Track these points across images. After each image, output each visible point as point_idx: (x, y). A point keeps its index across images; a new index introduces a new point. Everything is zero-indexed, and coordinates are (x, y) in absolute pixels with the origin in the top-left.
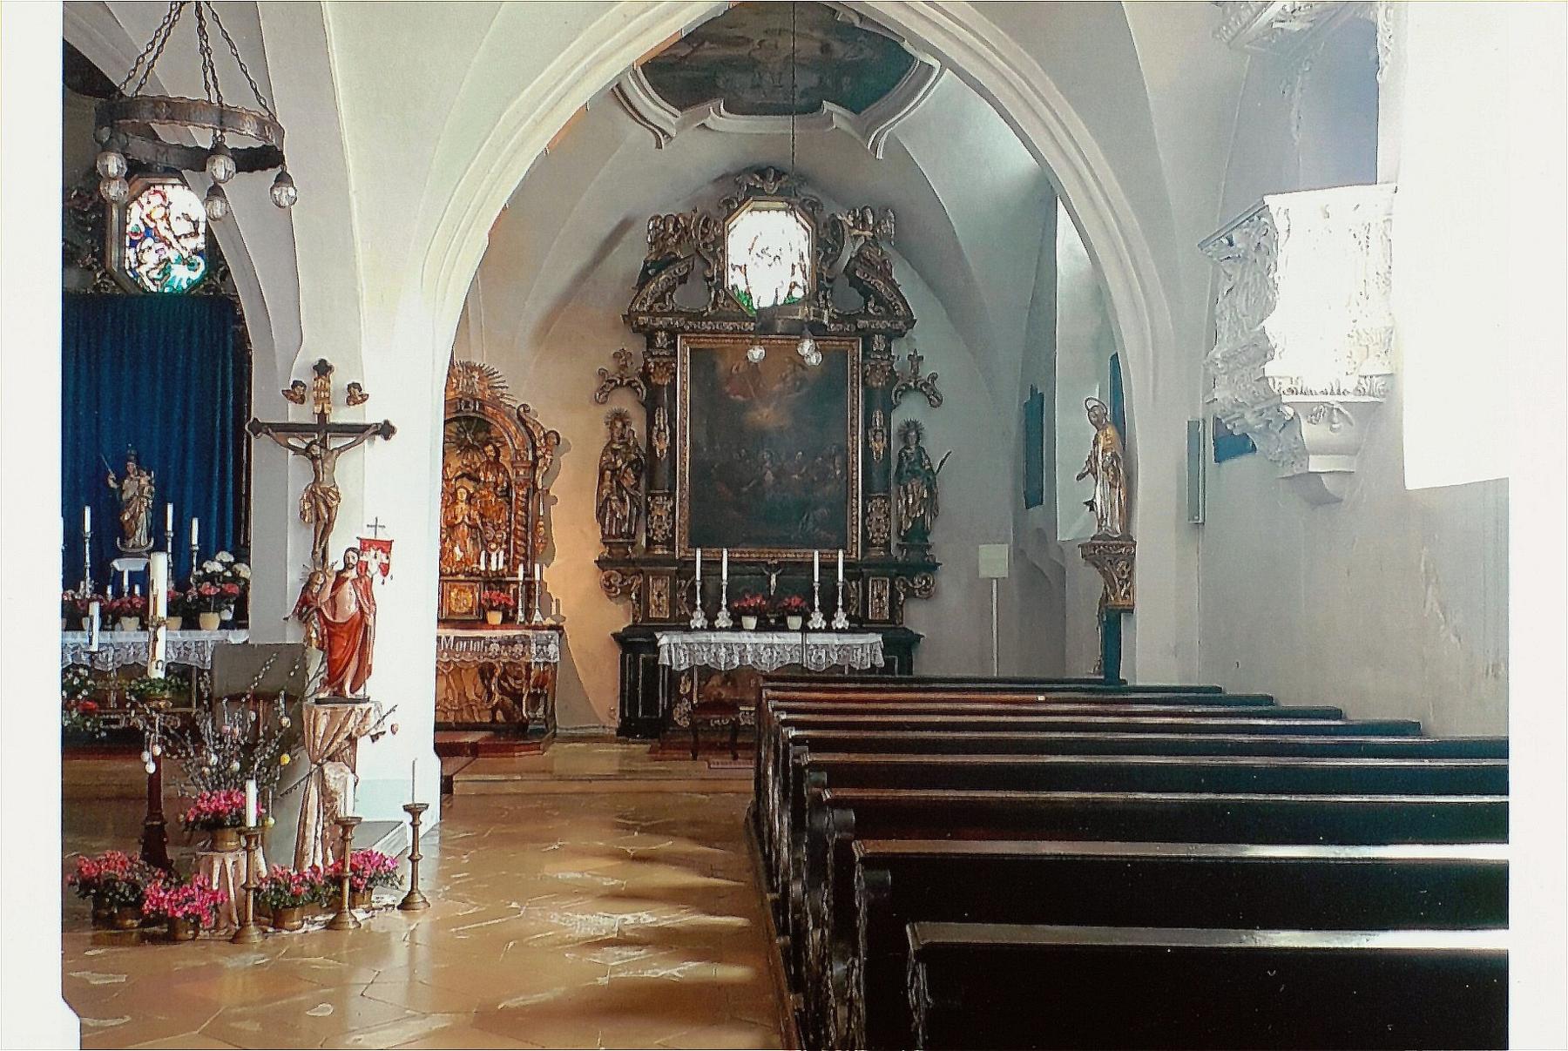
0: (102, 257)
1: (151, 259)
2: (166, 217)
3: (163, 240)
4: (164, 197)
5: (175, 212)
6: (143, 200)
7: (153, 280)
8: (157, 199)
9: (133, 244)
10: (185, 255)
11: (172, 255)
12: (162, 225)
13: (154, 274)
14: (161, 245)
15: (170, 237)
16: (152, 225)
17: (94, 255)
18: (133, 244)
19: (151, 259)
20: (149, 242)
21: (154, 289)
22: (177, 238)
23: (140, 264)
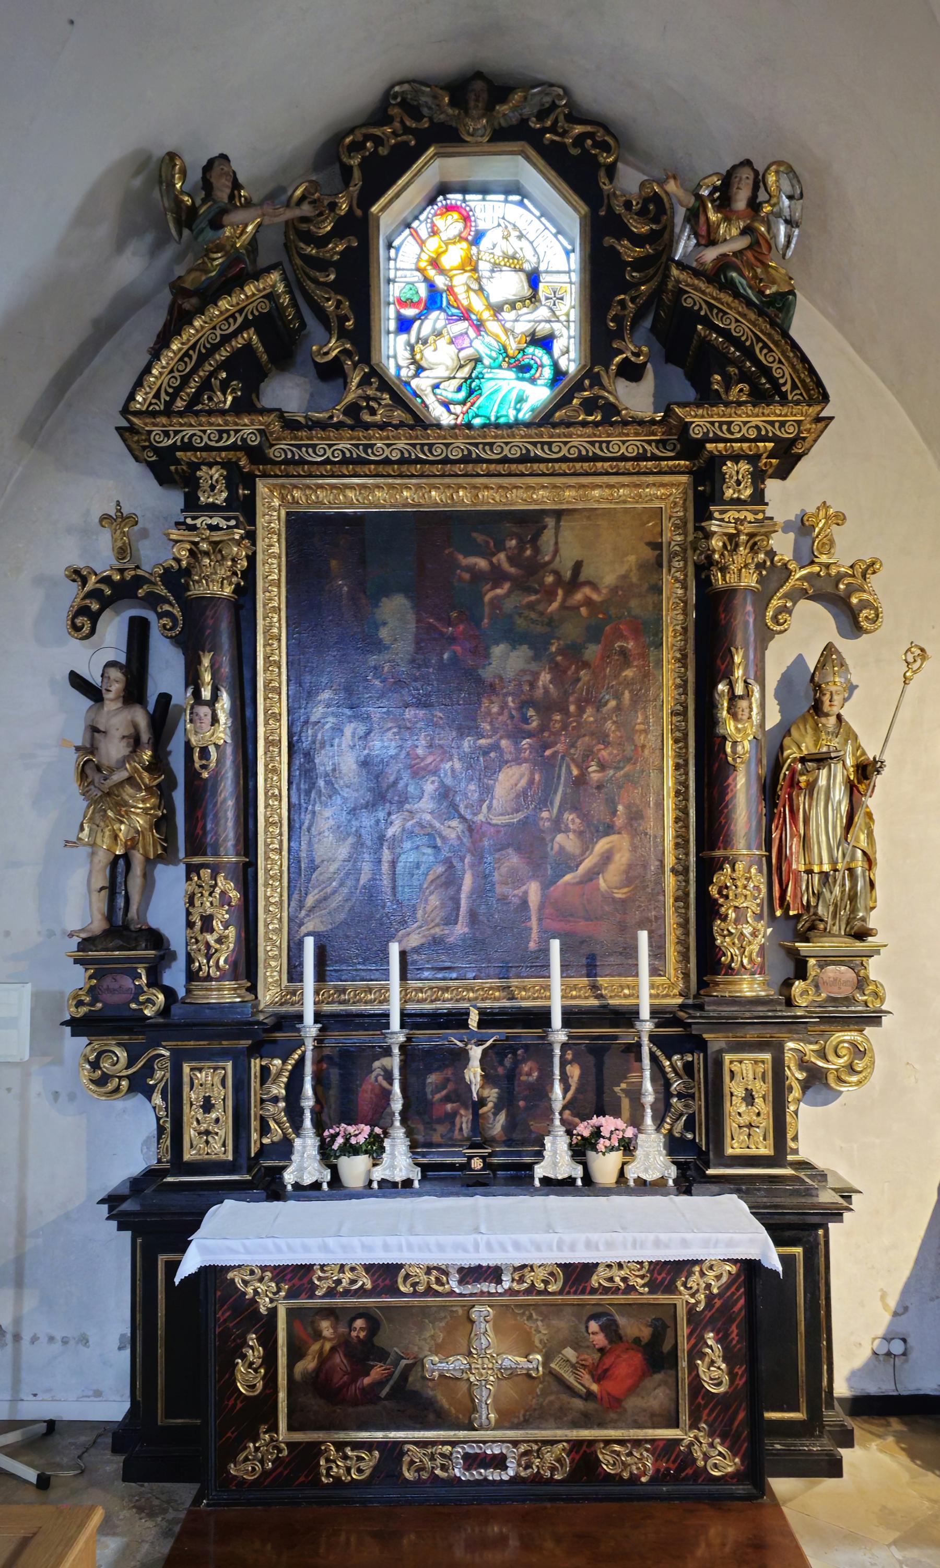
0: (362, 339)
1: (441, 358)
2: (470, 265)
3: (465, 315)
4: (466, 219)
5: (494, 243)
6: (422, 229)
7: (446, 404)
8: (450, 225)
9: (404, 325)
10: (512, 346)
11: (482, 346)
12: (460, 281)
13: (449, 390)
14: (463, 325)
15: (478, 305)
16: (440, 282)
17: (343, 334)
18: (404, 325)
19: (441, 358)
20: (436, 319)
21: (447, 420)
22: (497, 310)
23: (420, 369)
